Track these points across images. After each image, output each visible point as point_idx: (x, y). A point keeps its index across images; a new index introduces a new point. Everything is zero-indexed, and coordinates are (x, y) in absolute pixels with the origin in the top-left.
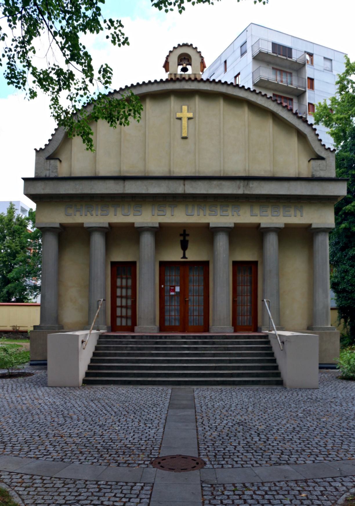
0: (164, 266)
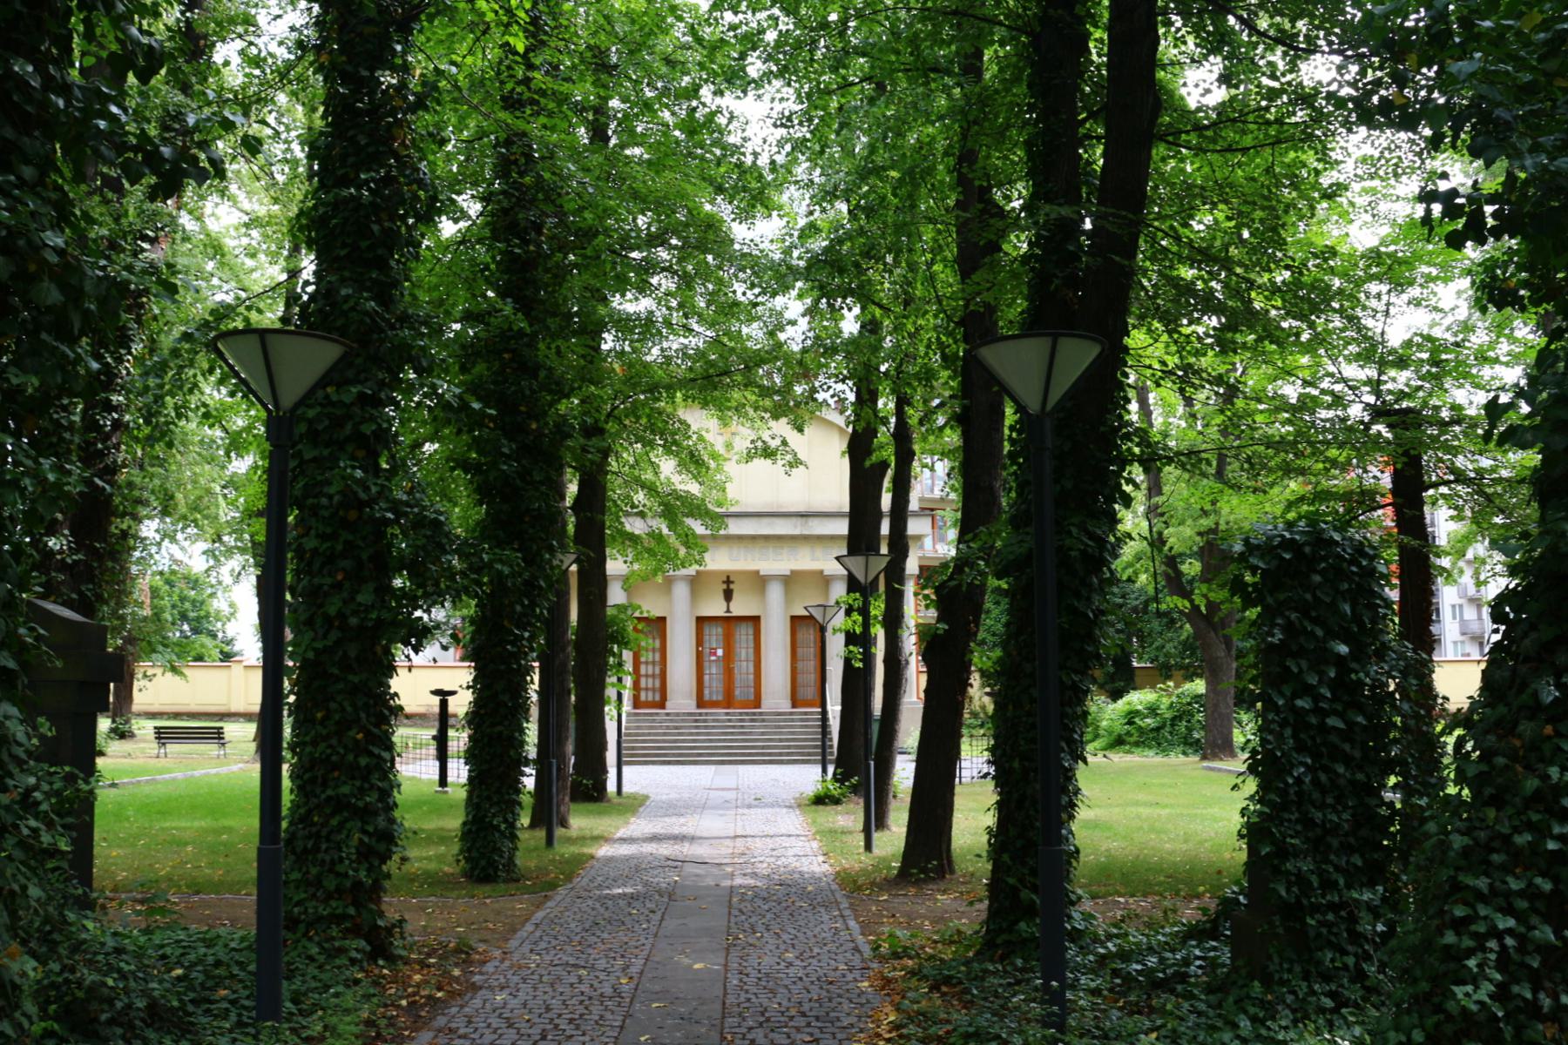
0: (701, 621)
